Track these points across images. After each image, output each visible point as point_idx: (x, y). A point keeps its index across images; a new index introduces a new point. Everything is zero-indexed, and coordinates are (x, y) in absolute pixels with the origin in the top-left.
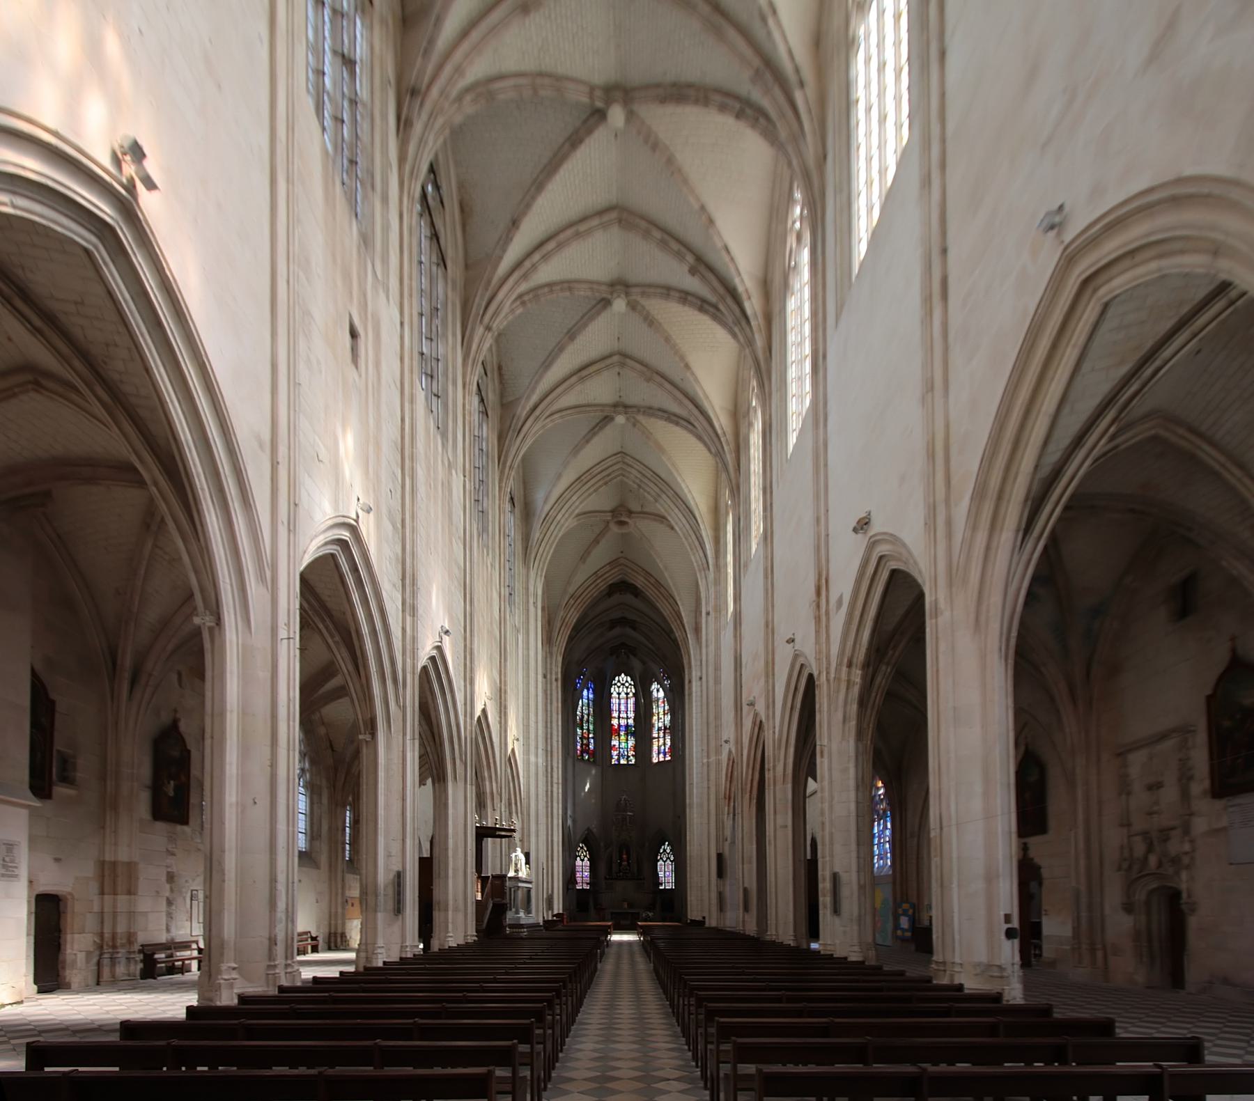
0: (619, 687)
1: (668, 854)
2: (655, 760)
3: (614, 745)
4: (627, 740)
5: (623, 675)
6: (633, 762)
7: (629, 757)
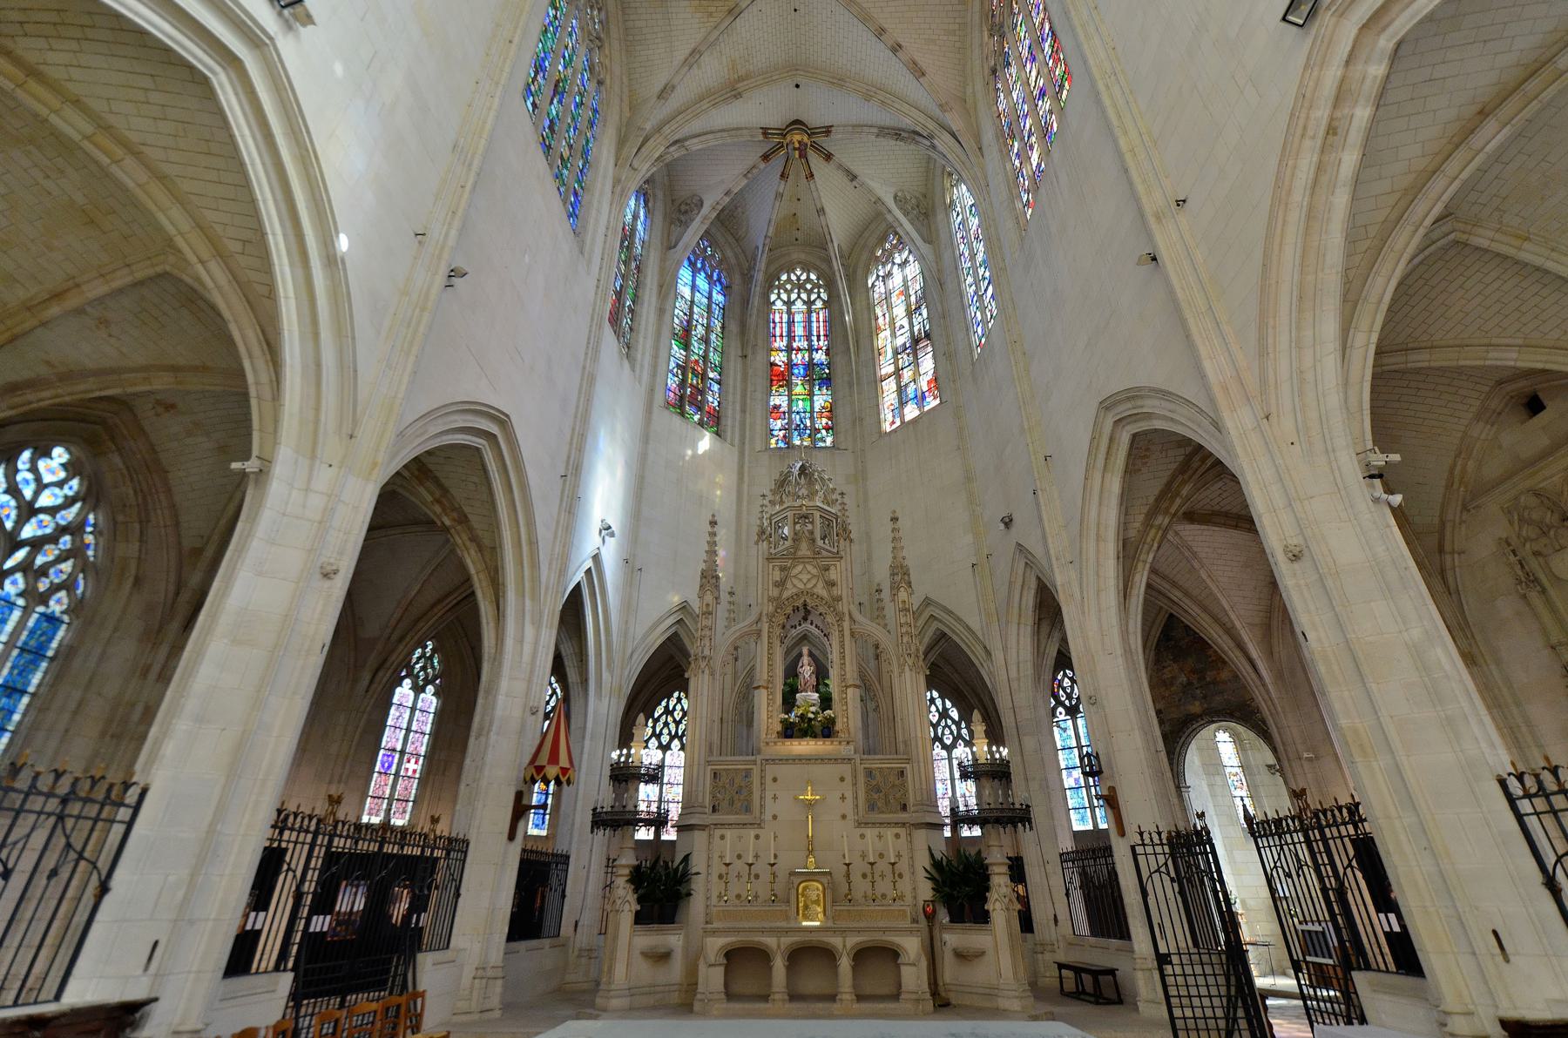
0: (789, 292)
2: (887, 427)
3: (777, 407)
4: (811, 394)
5: (798, 273)
6: (829, 440)
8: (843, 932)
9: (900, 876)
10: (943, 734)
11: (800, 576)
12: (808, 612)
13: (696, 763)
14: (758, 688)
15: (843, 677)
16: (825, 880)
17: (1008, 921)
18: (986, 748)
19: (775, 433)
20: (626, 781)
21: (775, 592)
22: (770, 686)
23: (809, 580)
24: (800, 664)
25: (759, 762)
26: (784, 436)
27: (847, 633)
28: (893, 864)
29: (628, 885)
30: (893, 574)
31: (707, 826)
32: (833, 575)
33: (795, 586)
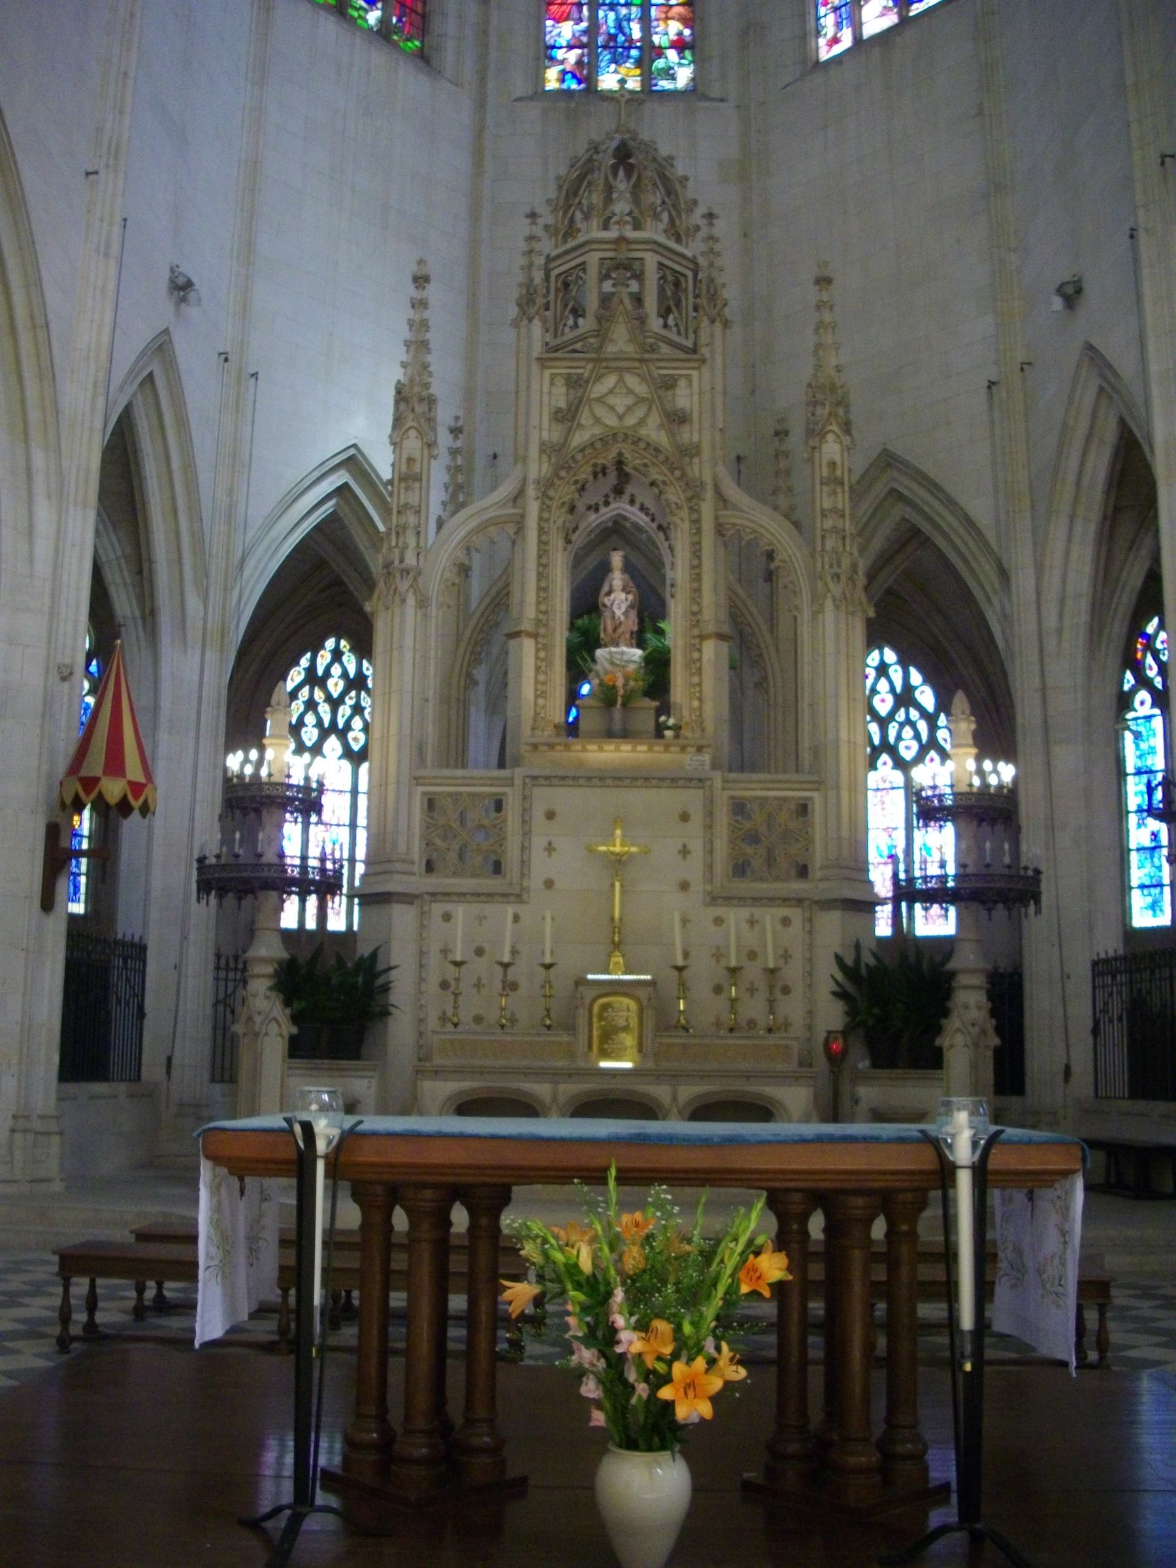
1: (883, 723)
6: (684, 76)
7: (659, 52)
8: (674, 1077)
9: (786, 990)
10: (899, 738)
11: (611, 400)
12: (624, 477)
13: (392, 779)
14: (516, 635)
15: (695, 618)
16: (643, 993)
17: (974, 1067)
18: (971, 765)
19: (559, 54)
20: (258, 811)
21: (553, 433)
22: (542, 631)
23: (629, 409)
24: (606, 588)
25: (518, 781)
26: (579, 63)
27: (708, 525)
28: (772, 971)
29: (273, 994)
30: (814, 403)
31: (416, 896)
32: (683, 398)
33: (598, 421)
